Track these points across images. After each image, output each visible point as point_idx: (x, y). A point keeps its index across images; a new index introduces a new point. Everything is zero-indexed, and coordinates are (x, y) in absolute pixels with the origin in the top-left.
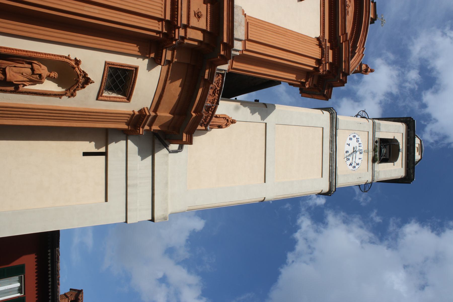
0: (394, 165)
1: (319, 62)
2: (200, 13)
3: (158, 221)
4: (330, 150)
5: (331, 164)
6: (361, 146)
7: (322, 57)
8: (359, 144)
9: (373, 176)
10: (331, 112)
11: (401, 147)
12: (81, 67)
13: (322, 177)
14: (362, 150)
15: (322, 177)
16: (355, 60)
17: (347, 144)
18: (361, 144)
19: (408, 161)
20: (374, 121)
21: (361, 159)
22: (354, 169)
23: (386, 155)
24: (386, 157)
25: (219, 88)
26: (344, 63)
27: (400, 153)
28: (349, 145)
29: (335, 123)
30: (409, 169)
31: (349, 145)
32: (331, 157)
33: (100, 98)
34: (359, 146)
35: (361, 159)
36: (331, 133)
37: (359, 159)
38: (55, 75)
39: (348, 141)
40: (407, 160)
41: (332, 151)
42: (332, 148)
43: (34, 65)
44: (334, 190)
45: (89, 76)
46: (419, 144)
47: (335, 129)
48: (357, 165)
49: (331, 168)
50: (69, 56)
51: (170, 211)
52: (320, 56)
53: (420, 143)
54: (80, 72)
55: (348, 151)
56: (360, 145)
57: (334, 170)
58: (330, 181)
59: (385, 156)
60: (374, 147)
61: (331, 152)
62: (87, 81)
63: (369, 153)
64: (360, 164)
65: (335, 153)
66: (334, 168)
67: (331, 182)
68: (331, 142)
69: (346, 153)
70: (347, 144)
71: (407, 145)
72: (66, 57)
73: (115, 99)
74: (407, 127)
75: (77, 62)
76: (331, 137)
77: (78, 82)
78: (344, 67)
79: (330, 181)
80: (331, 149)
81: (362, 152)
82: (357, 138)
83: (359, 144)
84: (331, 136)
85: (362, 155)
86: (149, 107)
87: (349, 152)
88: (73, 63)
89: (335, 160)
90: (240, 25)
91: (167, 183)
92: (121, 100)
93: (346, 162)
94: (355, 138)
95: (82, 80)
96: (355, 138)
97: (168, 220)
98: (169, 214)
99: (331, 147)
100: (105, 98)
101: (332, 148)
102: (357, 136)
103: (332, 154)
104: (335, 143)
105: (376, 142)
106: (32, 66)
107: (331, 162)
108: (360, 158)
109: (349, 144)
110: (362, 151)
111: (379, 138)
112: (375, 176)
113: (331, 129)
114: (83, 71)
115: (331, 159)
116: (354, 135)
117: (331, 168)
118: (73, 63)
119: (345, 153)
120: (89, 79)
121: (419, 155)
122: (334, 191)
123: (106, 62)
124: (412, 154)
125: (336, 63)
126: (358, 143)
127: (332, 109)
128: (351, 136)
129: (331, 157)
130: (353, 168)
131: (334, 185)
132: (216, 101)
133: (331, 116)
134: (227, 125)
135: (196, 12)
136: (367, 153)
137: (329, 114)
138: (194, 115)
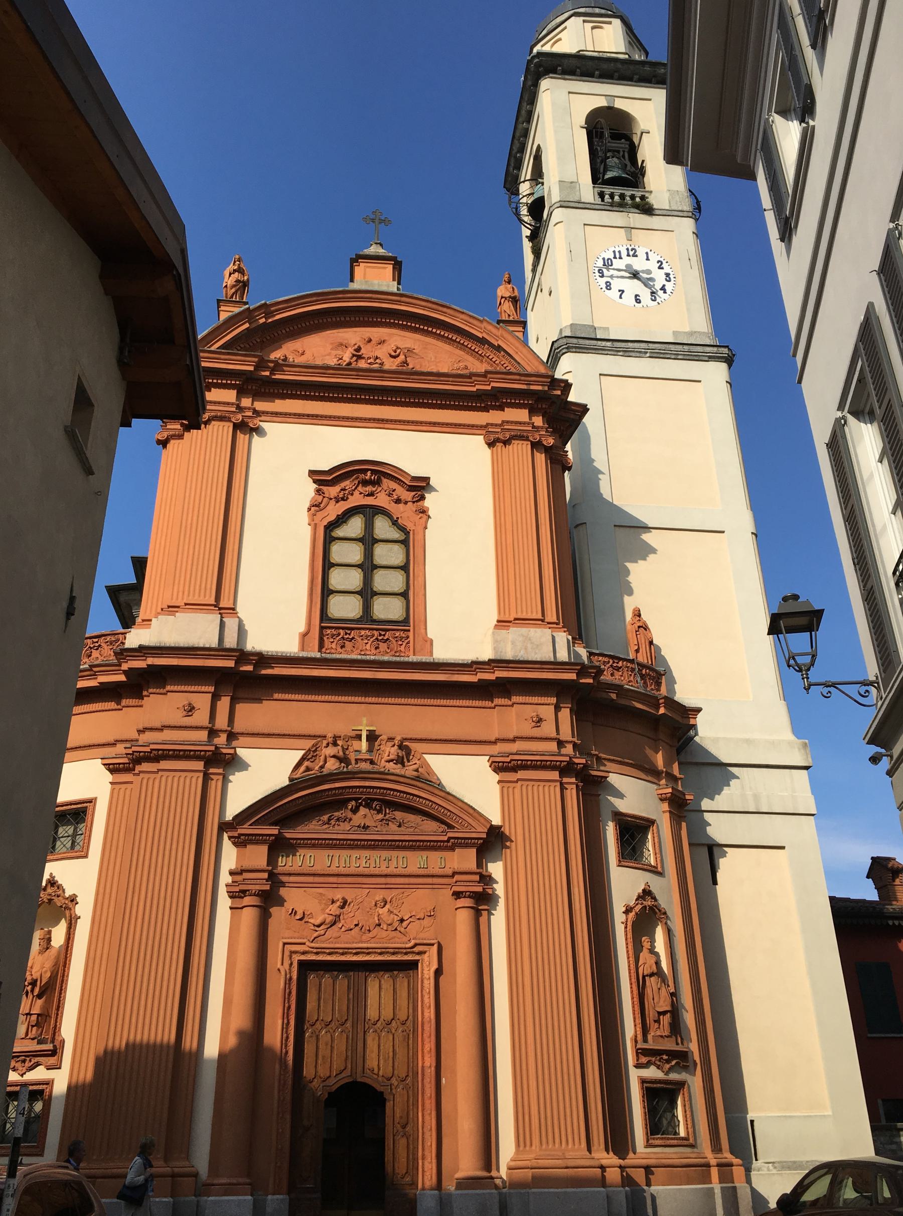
0: (649, 133)
1: (536, 446)
2: (534, 719)
3: (810, 760)
4: (643, 355)
5: (673, 357)
6: (620, 252)
7: (527, 439)
8: (615, 258)
9: (680, 214)
10: (564, 351)
11: (602, 102)
12: (632, 904)
13: (700, 381)
14: (628, 249)
15: (700, 381)
18: (614, 252)
19: (635, 79)
20: (558, 205)
21: (647, 253)
22: (671, 276)
23: (621, 150)
24: (626, 150)
25: (611, 661)
26: (532, 387)
27: (619, 104)
28: (623, 291)
29: (587, 342)
30: (654, 76)
31: (623, 291)
32: (658, 355)
33: (660, 869)
34: (620, 258)
35: (647, 253)
36: (609, 353)
37: (648, 259)
38: (648, 942)
39: (614, 294)
40: (631, 79)
41: (646, 353)
42: (640, 352)
43: (645, 973)
44: (726, 350)
45: (641, 891)
46: (584, 21)
47: (599, 342)
48: (662, 268)
49: (680, 357)
50: (623, 923)
51: (792, 737)
53: (579, 16)
54: (637, 904)
55: (636, 296)
56: (618, 256)
57: (686, 347)
58: (706, 359)
59: (624, 151)
60: (617, 209)
61: (648, 355)
62: (647, 893)
63: (632, 226)
64: (662, 259)
65: (651, 345)
66: (679, 348)
67: (710, 357)
68: (627, 354)
69: (640, 302)
71: (596, 78)
72: (626, 927)
73: (657, 845)
74: (551, 75)
75: (628, 911)
77: (651, 908)
78: (540, 388)
79: (706, 359)
80: (640, 354)
81: (632, 250)
83: (615, 258)
84: (615, 352)
85: (641, 252)
86: (655, 787)
87: (637, 293)
88: (632, 915)
89: (663, 346)
90: (530, 639)
91: (748, 741)
92: (655, 835)
93: (659, 304)
95: (649, 902)
97: (807, 741)
98: (796, 739)
99: (638, 355)
100: (659, 859)
101: (640, 352)
102: (600, 263)
103: (651, 352)
104: (630, 345)
105: (602, 195)
106: (647, 976)
107: (668, 356)
109: (619, 291)
110: (630, 248)
111: (594, 187)
112: (680, 209)
113: (601, 352)
114: (636, 900)
115: (661, 356)
116: (597, 274)
117: (680, 357)
118: (632, 915)
119: (640, 305)
120: (644, 890)
121: (610, 23)
122: (729, 349)
123: (619, 866)
124: (619, 66)
126: (613, 260)
127: (556, 345)
129: (658, 355)
130: (669, 281)
131: (715, 349)
132: (629, 665)
134: (646, 628)
135: (533, 724)
136: (633, 230)
138: (662, 711)
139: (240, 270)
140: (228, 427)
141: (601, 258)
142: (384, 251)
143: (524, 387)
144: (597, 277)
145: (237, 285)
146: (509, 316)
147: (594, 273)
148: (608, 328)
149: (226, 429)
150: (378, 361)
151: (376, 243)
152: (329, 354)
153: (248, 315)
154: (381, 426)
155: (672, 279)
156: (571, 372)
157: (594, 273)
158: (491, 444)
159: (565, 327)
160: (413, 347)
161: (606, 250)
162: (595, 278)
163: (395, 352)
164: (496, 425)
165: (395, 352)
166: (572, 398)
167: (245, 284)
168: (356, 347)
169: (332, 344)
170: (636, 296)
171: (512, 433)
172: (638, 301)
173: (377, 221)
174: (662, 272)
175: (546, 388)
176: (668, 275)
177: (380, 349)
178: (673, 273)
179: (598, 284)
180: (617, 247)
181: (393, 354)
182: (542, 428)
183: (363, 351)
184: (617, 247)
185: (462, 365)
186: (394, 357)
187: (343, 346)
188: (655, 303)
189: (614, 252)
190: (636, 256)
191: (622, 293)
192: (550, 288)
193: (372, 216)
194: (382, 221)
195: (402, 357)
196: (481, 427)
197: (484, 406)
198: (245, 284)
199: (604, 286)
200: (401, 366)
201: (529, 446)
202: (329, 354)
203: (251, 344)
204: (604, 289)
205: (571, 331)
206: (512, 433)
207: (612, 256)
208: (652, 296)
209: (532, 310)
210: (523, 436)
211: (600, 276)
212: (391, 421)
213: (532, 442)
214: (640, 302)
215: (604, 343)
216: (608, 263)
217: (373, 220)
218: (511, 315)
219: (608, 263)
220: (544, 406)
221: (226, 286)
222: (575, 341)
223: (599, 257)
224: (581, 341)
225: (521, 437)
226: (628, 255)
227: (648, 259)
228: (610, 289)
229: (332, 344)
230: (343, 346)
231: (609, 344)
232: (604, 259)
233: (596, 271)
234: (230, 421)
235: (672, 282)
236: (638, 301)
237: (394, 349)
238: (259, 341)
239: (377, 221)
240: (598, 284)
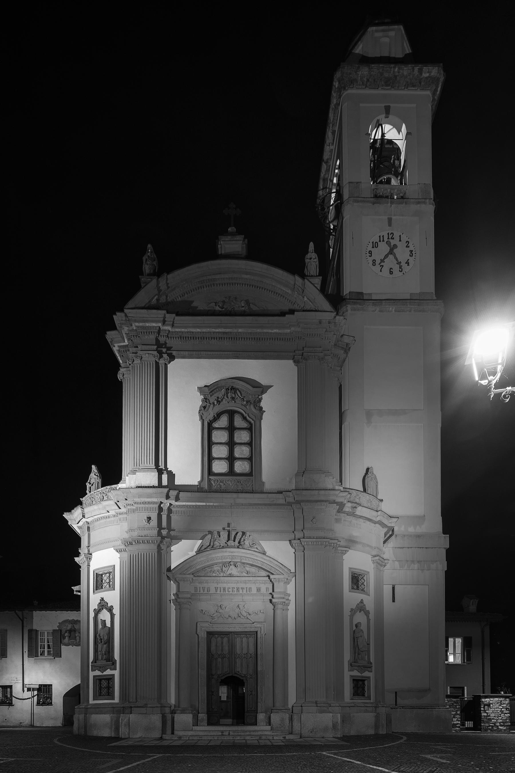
6: (383, 236)
14: (388, 234)
17: (381, 271)
18: (380, 236)
21: (400, 236)
35: (400, 236)
37: (400, 241)
56: (382, 240)
70: (381, 271)
83: (380, 241)
94: (372, 250)
96: (372, 250)
102: (370, 248)
108: (399, 240)
116: (368, 255)
126: (379, 243)
128: (370, 260)
147: (366, 254)
155: (414, 255)
157: (366, 254)
162: (367, 257)
170: (390, 269)
172: (391, 273)
174: (408, 249)
176: (411, 251)
178: (415, 250)
188: (401, 274)
189: (380, 236)
190: (393, 239)
199: (371, 263)
208: (400, 268)
214: (392, 273)
226: (388, 238)
227: (400, 241)
232: (373, 243)
233: (368, 253)
235: (414, 257)
236: (391, 273)
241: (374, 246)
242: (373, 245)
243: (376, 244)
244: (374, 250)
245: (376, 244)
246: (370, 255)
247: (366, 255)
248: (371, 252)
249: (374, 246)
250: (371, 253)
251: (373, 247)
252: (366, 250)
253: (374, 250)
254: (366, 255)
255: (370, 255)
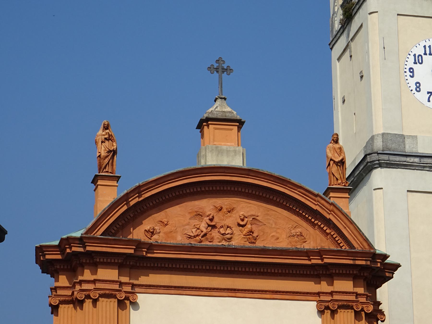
1: (357, 314)
6: (430, 47)
7: (352, 308)
8: (425, 54)
16: (345, 228)
17: (429, 101)
18: (425, 47)
29: (398, 158)
47: (408, 159)
52: (350, 311)
56: (428, 52)
70: (429, 101)
76: (422, 169)
78: (363, 263)
82: (415, 63)
83: (425, 54)
94: (414, 66)
96: (414, 66)
116: (408, 74)
125: (355, 272)
126: (424, 56)
127: (369, 159)
128: (412, 82)
133: (385, 165)
137: (379, 169)
139: (109, 138)
140: (113, 303)
141: (412, 54)
142: (229, 109)
143: (351, 262)
144: (408, 77)
145: (109, 156)
146: (337, 179)
147: (405, 72)
148: (417, 136)
149: (113, 303)
150: (229, 231)
151: (221, 98)
152: (188, 224)
153: (125, 198)
154: (233, 294)
156: (382, 188)
157: (405, 72)
158: (321, 312)
159: (378, 135)
160: (256, 214)
161: (418, 45)
163: (243, 220)
164: (326, 293)
165: (243, 220)
166: (388, 261)
167: (114, 152)
168: (211, 217)
169: (190, 213)
171: (340, 303)
173: (220, 70)
175: (369, 263)
177: (230, 217)
179: (407, 59)
180: (427, 40)
181: (242, 223)
182: (364, 295)
183: (216, 219)
184: (427, 40)
185: (298, 230)
186: (243, 226)
187: (199, 215)
189: (425, 47)
191: (430, 96)
192: (361, 80)
193: (216, 65)
194: (224, 70)
195: (249, 226)
196: (314, 294)
197: (317, 275)
198: (114, 152)
199: (414, 87)
200: (248, 235)
201: (353, 314)
202: (188, 224)
203: (126, 220)
204: (414, 91)
205: (383, 141)
206: (340, 303)
207: (422, 53)
209: (339, 59)
210: (349, 306)
211: (410, 76)
212: (242, 290)
213: (355, 311)
215: (412, 160)
216: (419, 60)
217: (217, 69)
218: (339, 178)
219: (419, 60)
220: (365, 274)
221: (100, 156)
222: (386, 157)
223: (410, 53)
224: (392, 158)
225: (346, 306)
228: (419, 91)
229: (190, 213)
230: (199, 215)
231: (417, 160)
232: (415, 55)
233: (407, 70)
234: (116, 298)
237: (242, 217)
238: (132, 216)
239: (220, 70)
240: (407, 59)
241: (417, 61)
242: (415, 60)
243: (420, 57)
244: (416, 67)
245: (420, 57)
246: (412, 75)
247: (405, 73)
248: (411, 70)
249: (417, 61)
250: (413, 72)
251: (415, 63)
252: (405, 66)
253: (416, 67)
254: (405, 74)
255: (411, 74)
